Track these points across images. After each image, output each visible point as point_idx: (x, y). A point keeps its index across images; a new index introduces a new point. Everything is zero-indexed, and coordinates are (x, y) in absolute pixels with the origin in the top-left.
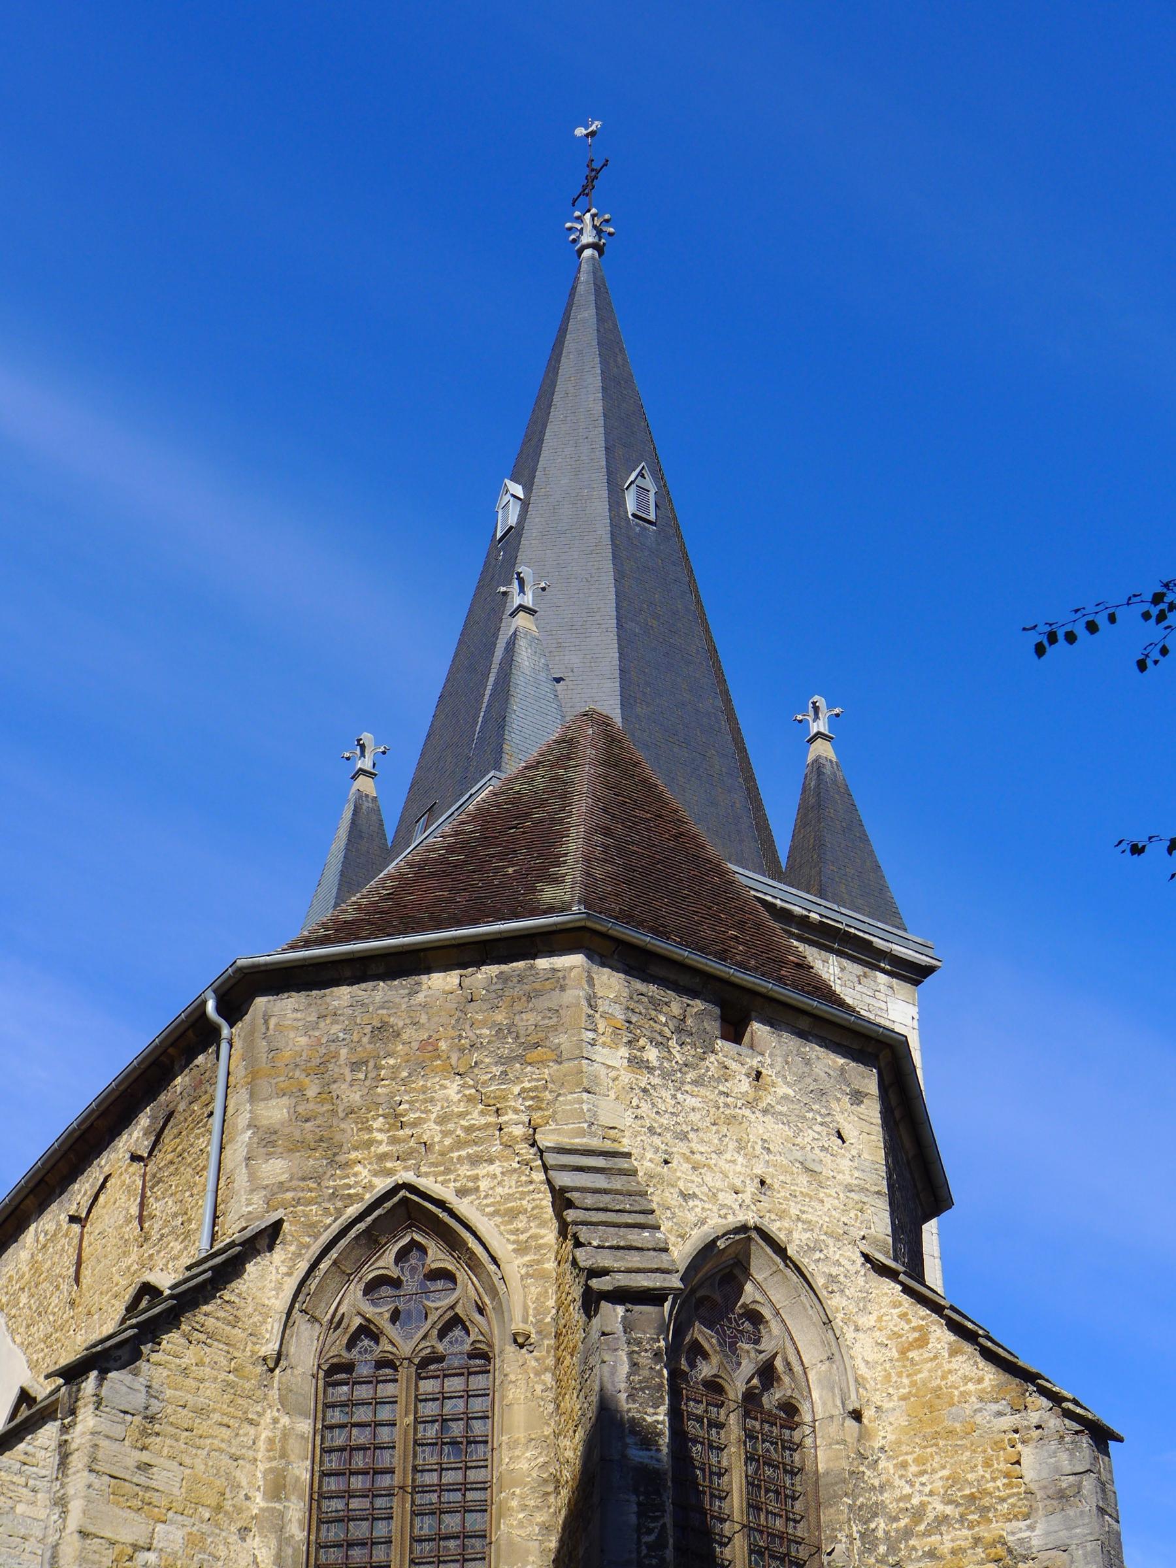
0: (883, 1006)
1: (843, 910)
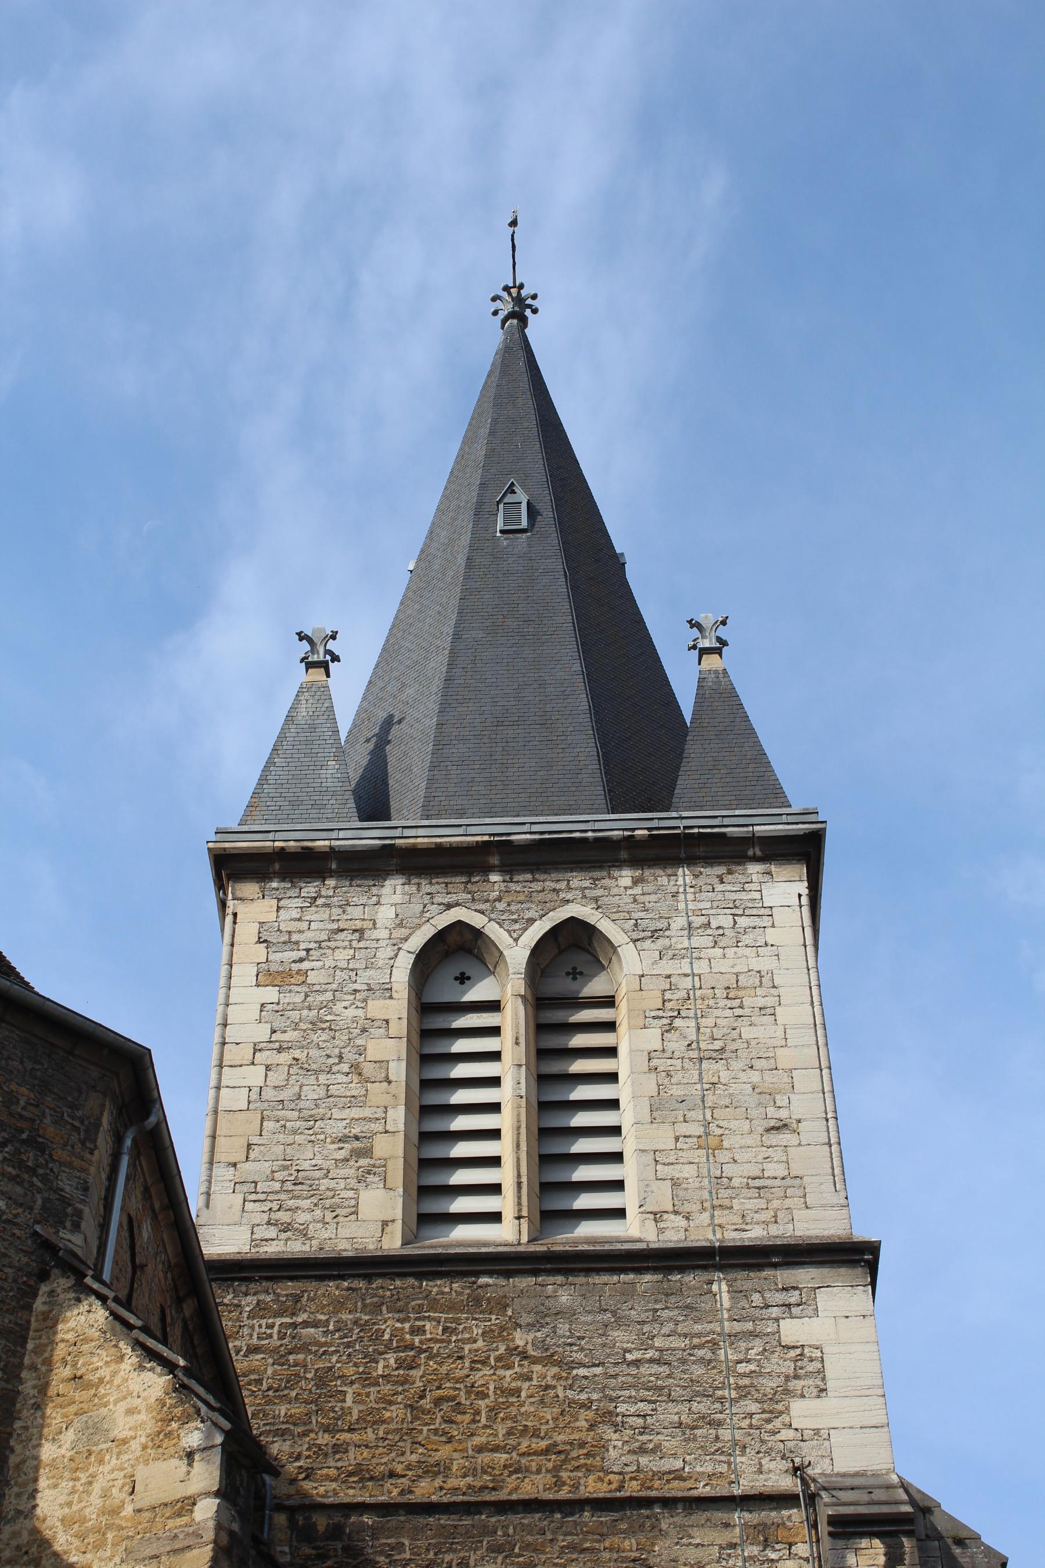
0: (757, 895)
1: (685, 814)
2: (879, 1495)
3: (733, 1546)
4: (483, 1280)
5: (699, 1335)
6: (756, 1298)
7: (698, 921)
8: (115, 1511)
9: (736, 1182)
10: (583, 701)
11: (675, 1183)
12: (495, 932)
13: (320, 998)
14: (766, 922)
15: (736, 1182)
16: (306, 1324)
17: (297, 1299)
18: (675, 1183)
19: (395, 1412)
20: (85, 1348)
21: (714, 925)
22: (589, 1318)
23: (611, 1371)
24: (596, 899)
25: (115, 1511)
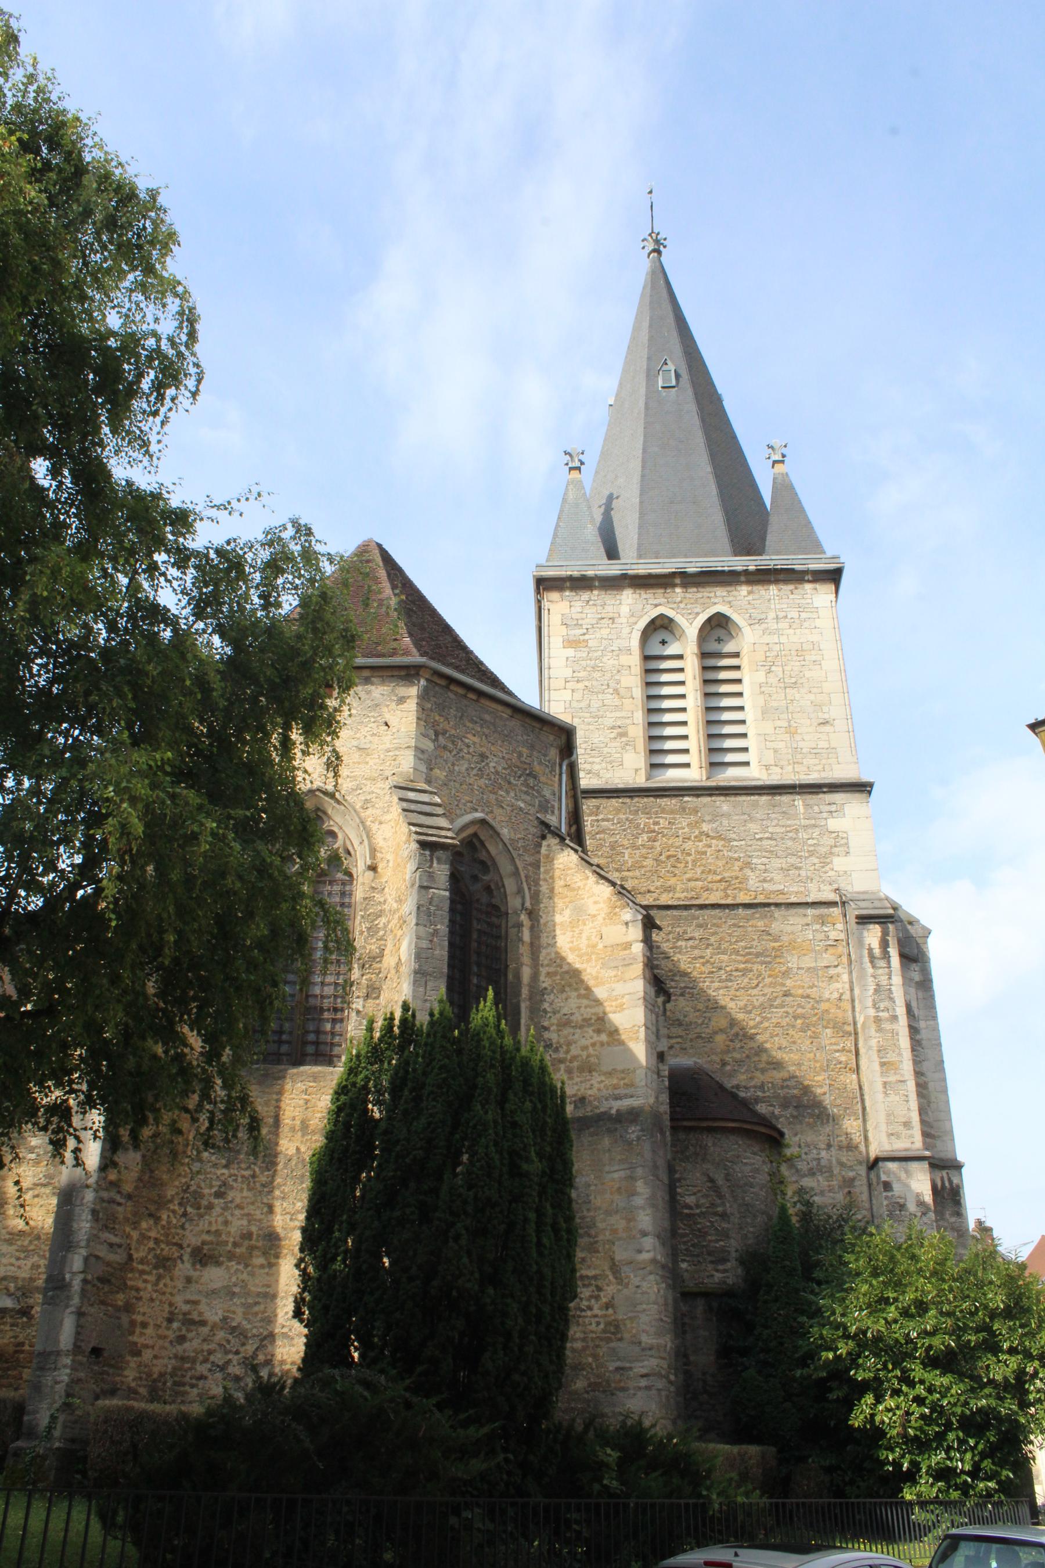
2: (877, 904)
3: (808, 925)
4: (686, 799)
5: (789, 826)
6: (816, 808)
7: (781, 614)
8: (594, 946)
9: (804, 751)
10: (713, 489)
11: (776, 751)
12: (679, 619)
13: (596, 654)
14: (815, 615)
15: (804, 751)
16: (603, 820)
17: (598, 808)
18: (776, 751)
19: (649, 862)
20: (569, 872)
21: (789, 616)
22: (737, 817)
23: (750, 843)
24: (730, 602)
25: (594, 946)
